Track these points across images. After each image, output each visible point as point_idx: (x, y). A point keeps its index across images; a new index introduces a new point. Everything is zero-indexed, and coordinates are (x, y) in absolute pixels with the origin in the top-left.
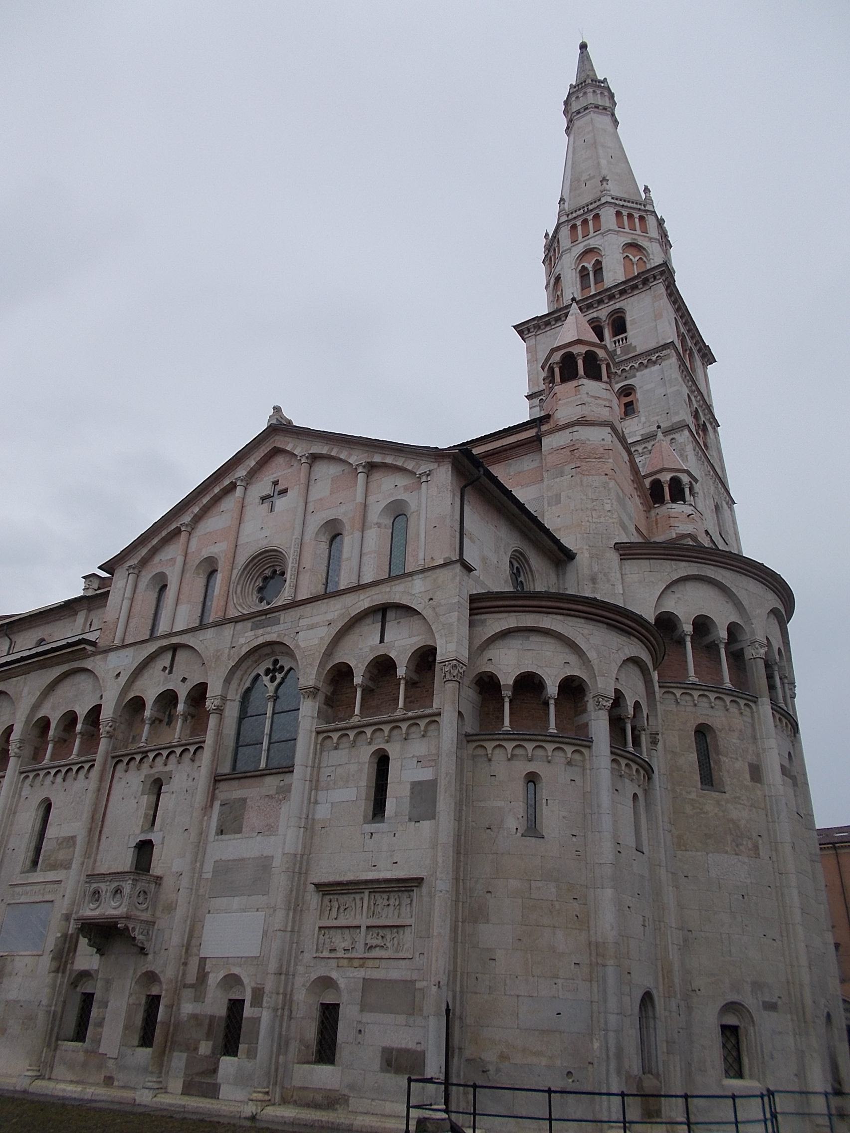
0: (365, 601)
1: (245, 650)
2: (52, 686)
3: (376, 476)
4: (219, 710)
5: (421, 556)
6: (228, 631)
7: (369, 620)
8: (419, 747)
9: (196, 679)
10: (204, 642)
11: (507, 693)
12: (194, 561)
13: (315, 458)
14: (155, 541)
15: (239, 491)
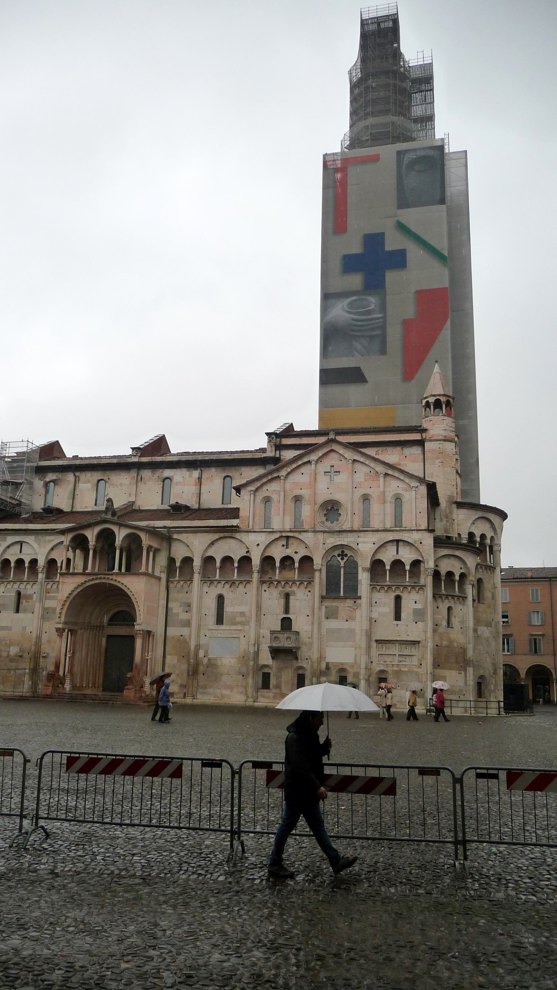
0: (391, 536)
1: (330, 546)
2: (212, 543)
3: (388, 479)
4: (320, 570)
5: (414, 523)
6: (320, 536)
7: (390, 544)
8: (415, 596)
9: (303, 552)
10: (308, 538)
11: (443, 578)
12: (290, 496)
13: (355, 461)
14: (265, 480)
15: (313, 466)
